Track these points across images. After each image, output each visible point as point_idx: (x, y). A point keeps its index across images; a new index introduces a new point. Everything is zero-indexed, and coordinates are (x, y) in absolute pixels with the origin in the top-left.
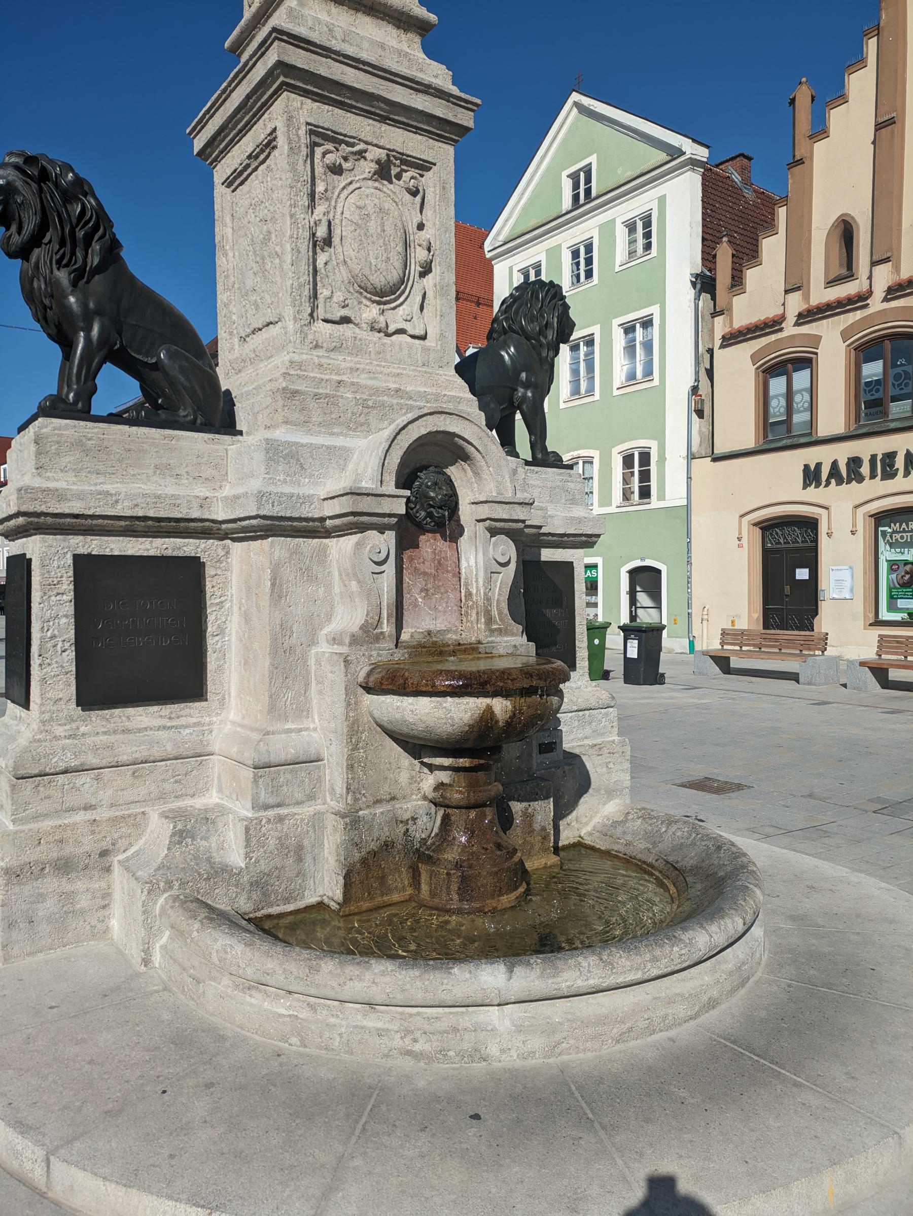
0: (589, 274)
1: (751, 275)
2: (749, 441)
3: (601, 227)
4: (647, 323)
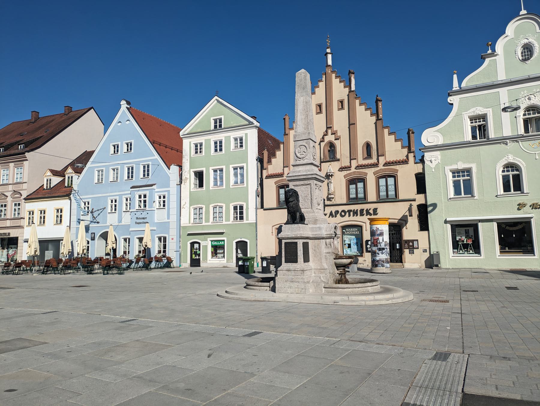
0: (221, 150)
1: (273, 160)
2: (275, 205)
3: (225, 137)
4: (241, 168)
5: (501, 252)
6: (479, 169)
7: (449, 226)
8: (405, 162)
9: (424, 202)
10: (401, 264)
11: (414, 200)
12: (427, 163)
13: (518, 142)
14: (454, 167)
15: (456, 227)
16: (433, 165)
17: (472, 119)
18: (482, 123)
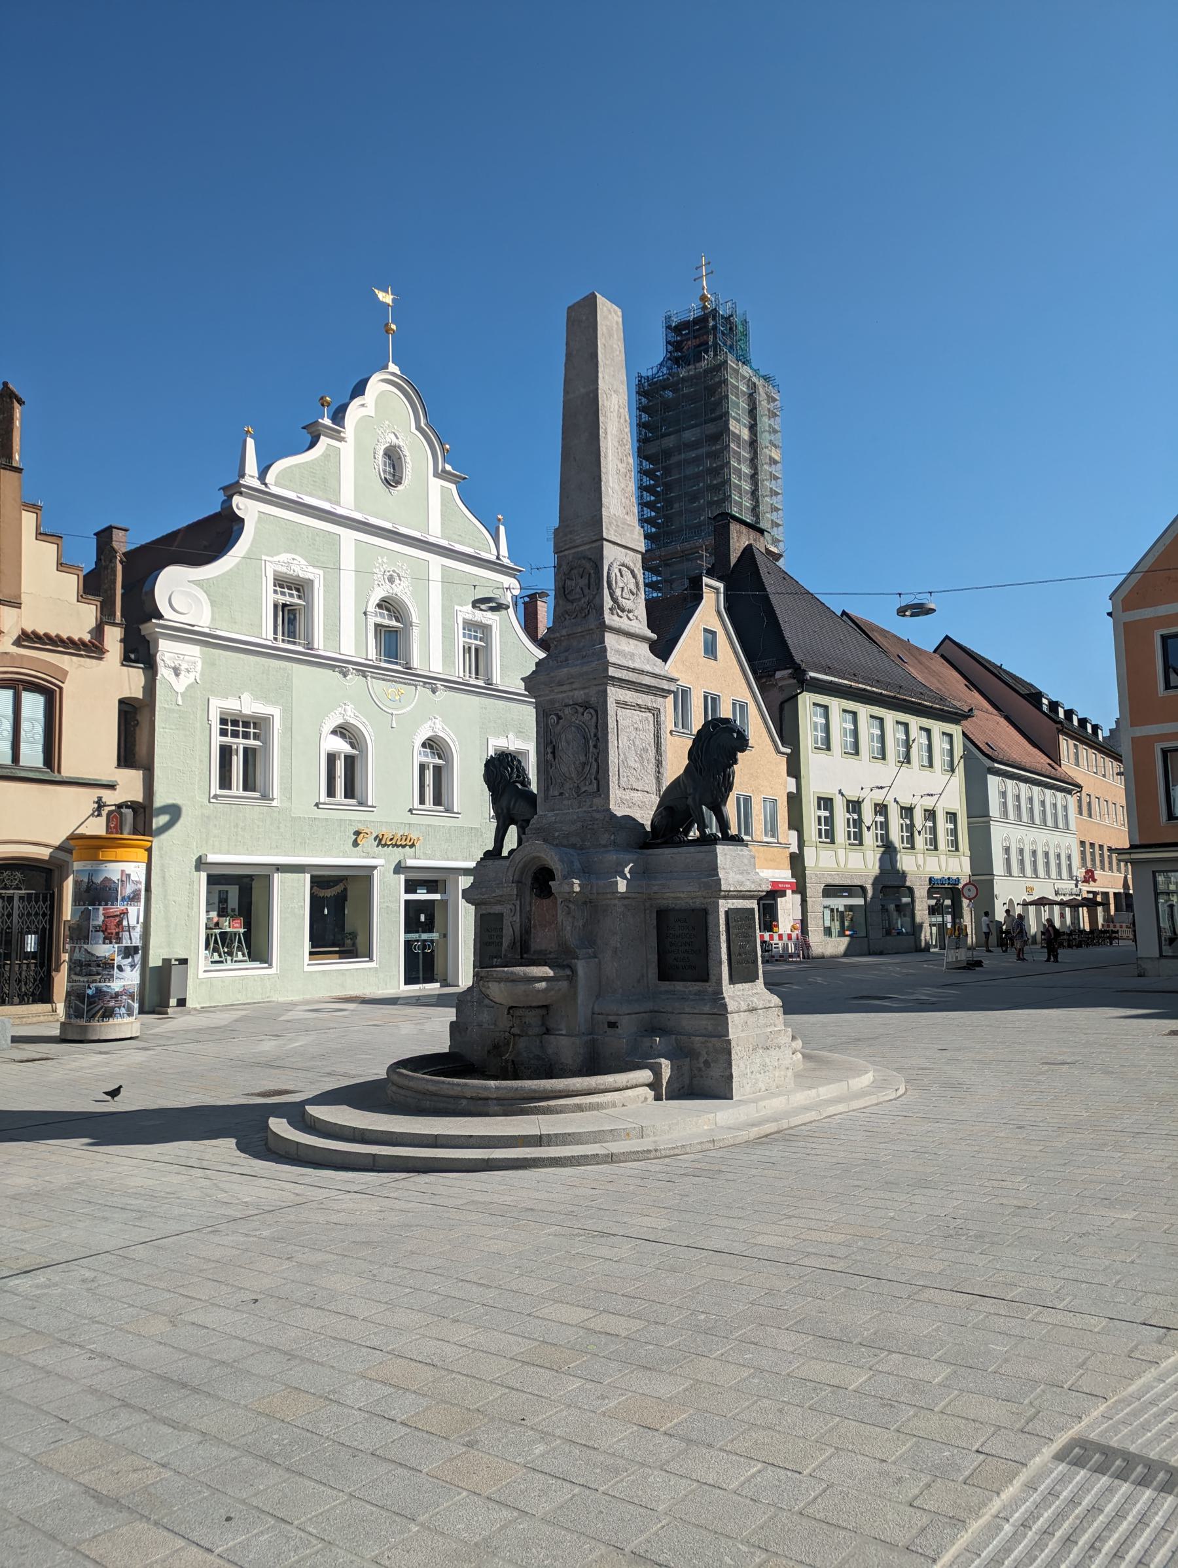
5: (311, 953)
6: (288, 729)
7: (203, 876)
8: (93, 648)
9: (139, 797)
10: (48, 1007)
11: (111, 787)
12: (164, 672)
13: (365, 677)
14: (232, 705)
15: (219, 880)
16: (181, 684)
17: (282, 582)
18: (296, 600)
